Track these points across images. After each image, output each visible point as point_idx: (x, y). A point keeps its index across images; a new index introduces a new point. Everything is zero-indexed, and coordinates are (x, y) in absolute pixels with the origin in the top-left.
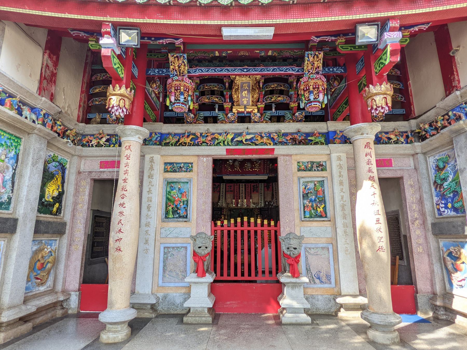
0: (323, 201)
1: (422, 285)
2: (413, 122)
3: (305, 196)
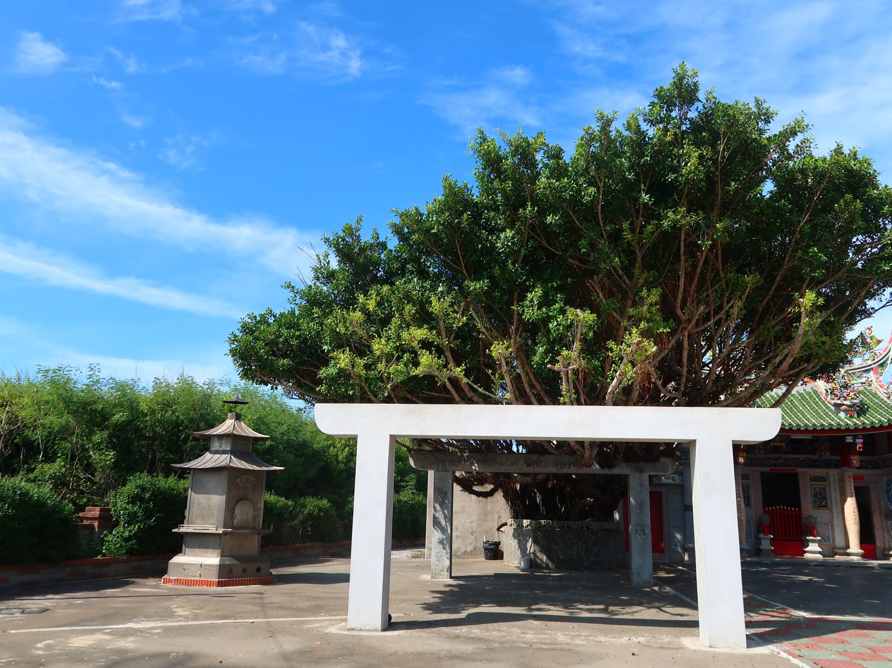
0: (825, 499)
1: (879, 544)
2: (875, 458)
3: (815, 495)
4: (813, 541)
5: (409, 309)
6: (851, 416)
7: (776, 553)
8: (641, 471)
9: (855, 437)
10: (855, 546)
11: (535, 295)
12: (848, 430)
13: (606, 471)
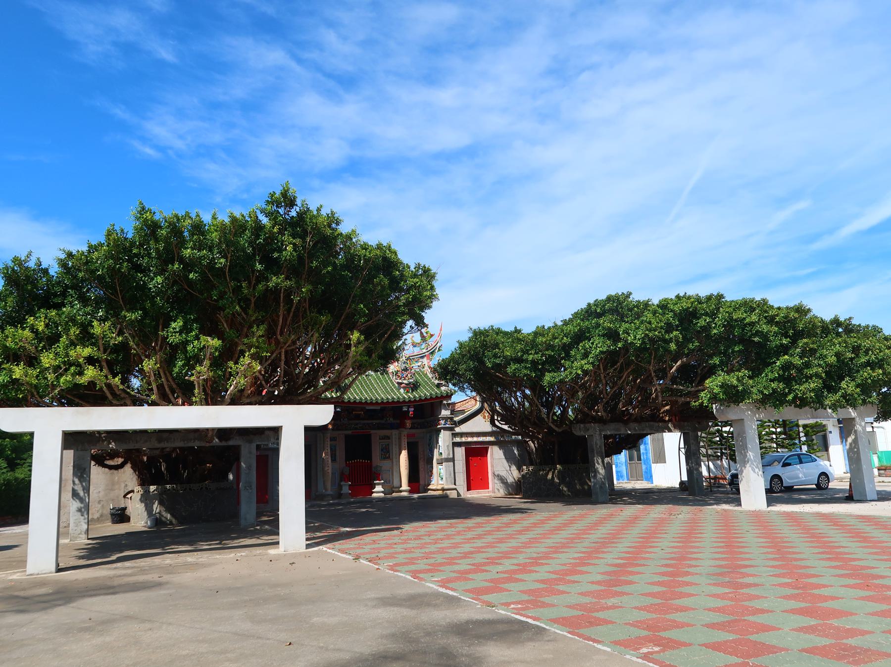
1: (422, 482)
4: (379, 484)
5: (74, 331)
6: (408, 392)
7: (352, 495)
8: (250, 442)
9: (409, 407)
10: (405, 486)
11: (177, 325)
12: (404, 402)
13: (224, 444)
